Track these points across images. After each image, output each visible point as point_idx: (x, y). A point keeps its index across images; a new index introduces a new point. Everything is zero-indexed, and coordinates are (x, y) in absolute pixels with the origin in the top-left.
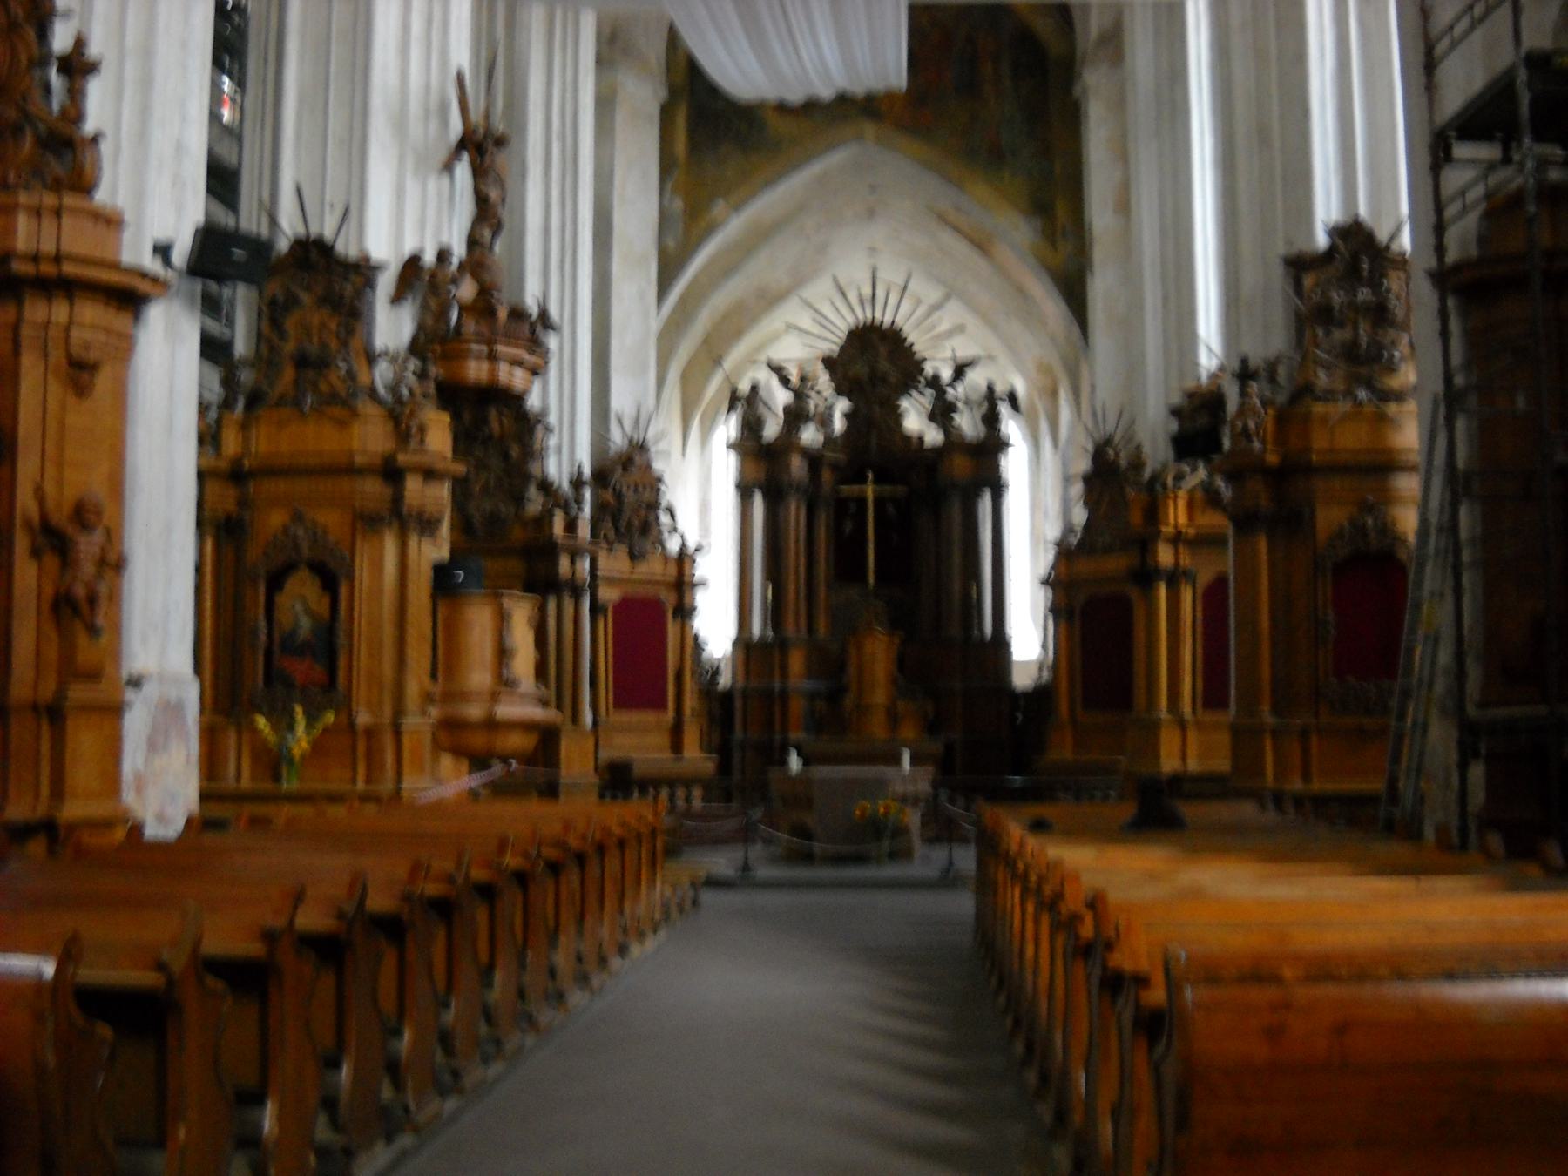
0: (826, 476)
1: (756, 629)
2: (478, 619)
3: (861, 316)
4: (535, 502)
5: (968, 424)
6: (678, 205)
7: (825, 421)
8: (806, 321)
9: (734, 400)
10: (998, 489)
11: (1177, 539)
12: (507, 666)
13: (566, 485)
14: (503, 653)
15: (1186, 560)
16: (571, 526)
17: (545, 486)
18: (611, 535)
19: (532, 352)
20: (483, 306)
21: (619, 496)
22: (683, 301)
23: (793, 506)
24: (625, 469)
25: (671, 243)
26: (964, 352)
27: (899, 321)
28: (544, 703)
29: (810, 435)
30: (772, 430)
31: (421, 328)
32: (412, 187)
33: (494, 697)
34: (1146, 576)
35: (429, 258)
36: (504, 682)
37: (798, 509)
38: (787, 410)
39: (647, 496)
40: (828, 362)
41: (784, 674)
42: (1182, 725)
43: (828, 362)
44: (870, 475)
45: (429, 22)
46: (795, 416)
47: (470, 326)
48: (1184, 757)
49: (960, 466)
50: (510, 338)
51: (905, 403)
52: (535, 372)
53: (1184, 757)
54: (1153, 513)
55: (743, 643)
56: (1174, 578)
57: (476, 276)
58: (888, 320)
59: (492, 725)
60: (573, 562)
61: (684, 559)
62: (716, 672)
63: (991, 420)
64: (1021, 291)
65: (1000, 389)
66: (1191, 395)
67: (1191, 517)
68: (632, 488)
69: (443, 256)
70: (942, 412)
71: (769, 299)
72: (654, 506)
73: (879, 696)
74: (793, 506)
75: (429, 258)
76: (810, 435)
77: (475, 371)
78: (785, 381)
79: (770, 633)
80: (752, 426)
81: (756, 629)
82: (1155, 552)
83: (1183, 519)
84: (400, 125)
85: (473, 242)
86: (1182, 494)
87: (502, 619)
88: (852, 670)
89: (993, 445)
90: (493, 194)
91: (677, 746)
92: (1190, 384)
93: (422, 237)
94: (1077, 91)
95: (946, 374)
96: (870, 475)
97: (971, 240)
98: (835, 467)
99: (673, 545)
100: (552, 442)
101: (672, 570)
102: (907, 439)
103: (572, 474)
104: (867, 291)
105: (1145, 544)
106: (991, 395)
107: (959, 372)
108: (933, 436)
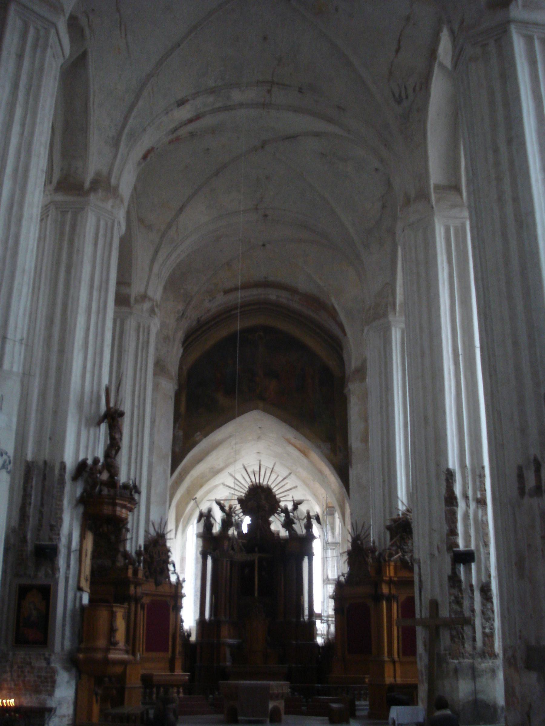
1: (207, 616)
2: (103, 614)
4: (121, 562)
6: (181, 433)
7: (238, 526)
8: (230, 482)
9: (201, 515)
10: (311, 556)
11: (390, 582)
12: (114, 637)
13: (133, 554)
14: (112, 630)
15: (393, 591)
16: (136, 572)
17: (126, 555)
19: (130, 502)
20: (112, 482)
22: (180, 474)
25: (177, 450)
26: (297, 498)
27: (269, 483)
28: (127, 652)
29: (232, 531)
30: (216, 529)
31: (85, 490)
32: (84, 433)
33: (107, 650)
34: (378, 598)
35: (90, 462)
36: (112, 644)
40: (240, 501)
42: (394, 662)
43: (241, 501)
44: (256, 549)
45: (94, 365)
46: (227, 523)
47: (105, 491)
48: (395, 677)
50: (122, 497)
52: (131, 510)
53: (395, 677)
54: (380, 571)
55: (201, 623)
56: (390, 599)
57: (109, 471)
59: (107, 662)
60: (135, 588)
61: (179, 585)
62: (189, 635)
63: (309, 526)
64: (321, 472)
66: (395, 521)
67: (396, 573)
69: (96, 461)
70: (288, 524)
71: (216, 472)
75: (90, 462)
76: (232, 531)
77: (107, 510)
78: (222, 508)
79: (213, 618)
80: (208, 526)
81: (207, 616)
82: (382, 589)
83: (392, 574)
84: (80, 406)
85: (107, 455)
86: (392, 564)
87: (113, 616)
89: (310, 537)
90: (117, 436)
91: (172, 669)
92: (395, 517)
93: (87, 455)
94: (346, 391)
95: (290, 507)
96: (256, 549)
97: (300, 450)
99: (173, 579)
100: (129, 536)
101: (173, 590)
102: (304, 556)
103: (136, 550)
105: (377, 585)
106: (309, 517)
107: (296, 505)
108: (284, 533)
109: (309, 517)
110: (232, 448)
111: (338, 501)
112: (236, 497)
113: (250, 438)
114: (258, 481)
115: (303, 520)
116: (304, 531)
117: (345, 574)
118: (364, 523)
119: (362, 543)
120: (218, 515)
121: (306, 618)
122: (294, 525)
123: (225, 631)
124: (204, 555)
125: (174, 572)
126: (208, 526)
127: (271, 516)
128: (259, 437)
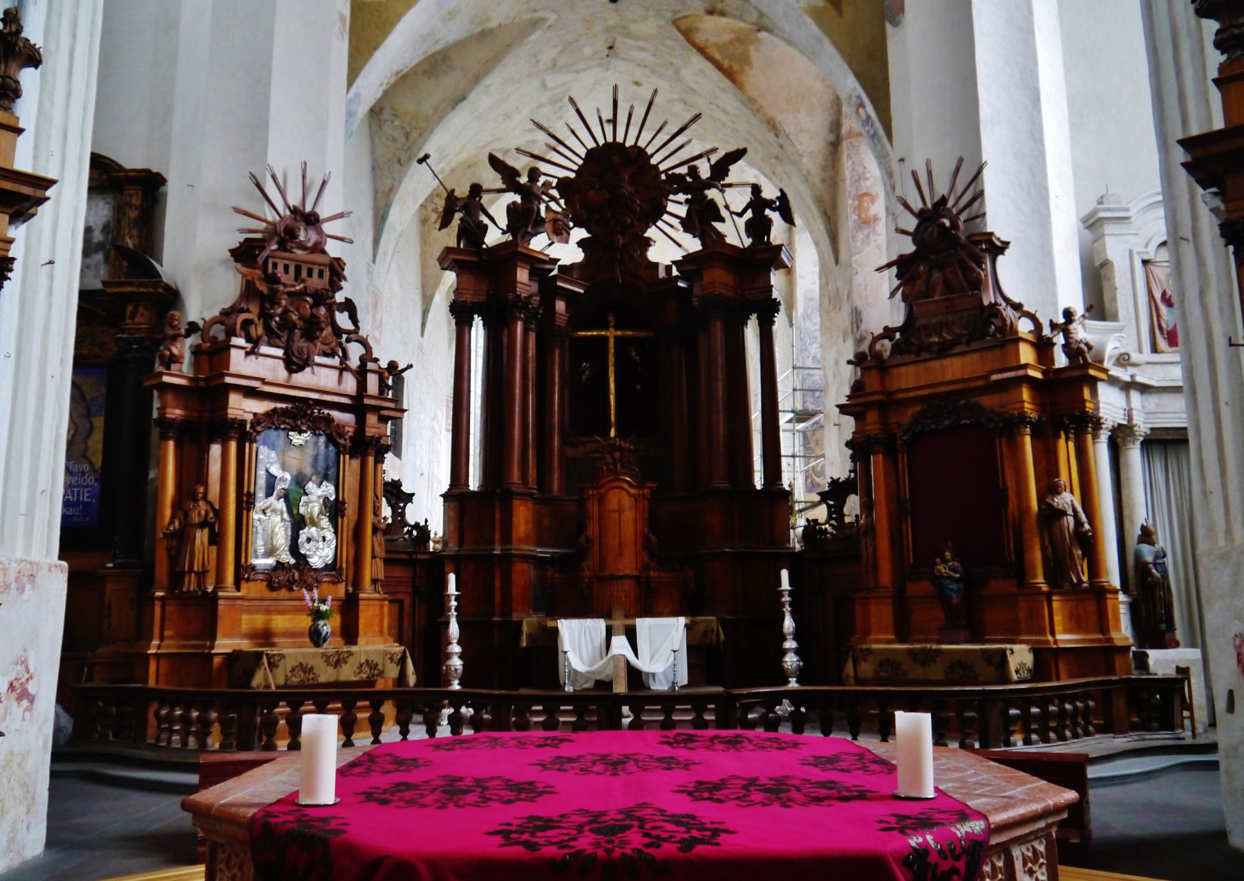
0: (560, 306)
1: (474, 484)
3: (601, 142)
5: (734, 233)
10: (767, 310)
18: (258, 330)
21: (272, 280)
23: (520, 325)
24: (283, 246)
27: (642, 144)
37: (526, 331)
38: (512, 210)
39: (316, 283)
41: (507, 538)
49: (719, 278)
51: (651, 232)
55: (456, 496)
58: (630, 143)
63: (759, 227)
65: (770, 192)
68: (292, 270)
72: (323, 298)
73: (627, 564)
74: (520, 325)
81: (474, 484)
88: (592, 530)
91: (350, 633)
98: (569, 296)
104: (607, 114)
109: (758, 203)
110: (544, 86)
111: (819, 201)
112: (555, 182)
113: (588, 51)
114: (610, 139)
115: (740, 215)
116: (748, 242)
117: (895, 330)
118: (961, 160)
119: (954, 225)
120: (499, 207)
121: (758, 482)
122: (717, 225)
123: (523, 517)
124: (461, 313)
125: (354, 335)
126: (473, 232)
127: (648, 227)
128: (611, 48)
